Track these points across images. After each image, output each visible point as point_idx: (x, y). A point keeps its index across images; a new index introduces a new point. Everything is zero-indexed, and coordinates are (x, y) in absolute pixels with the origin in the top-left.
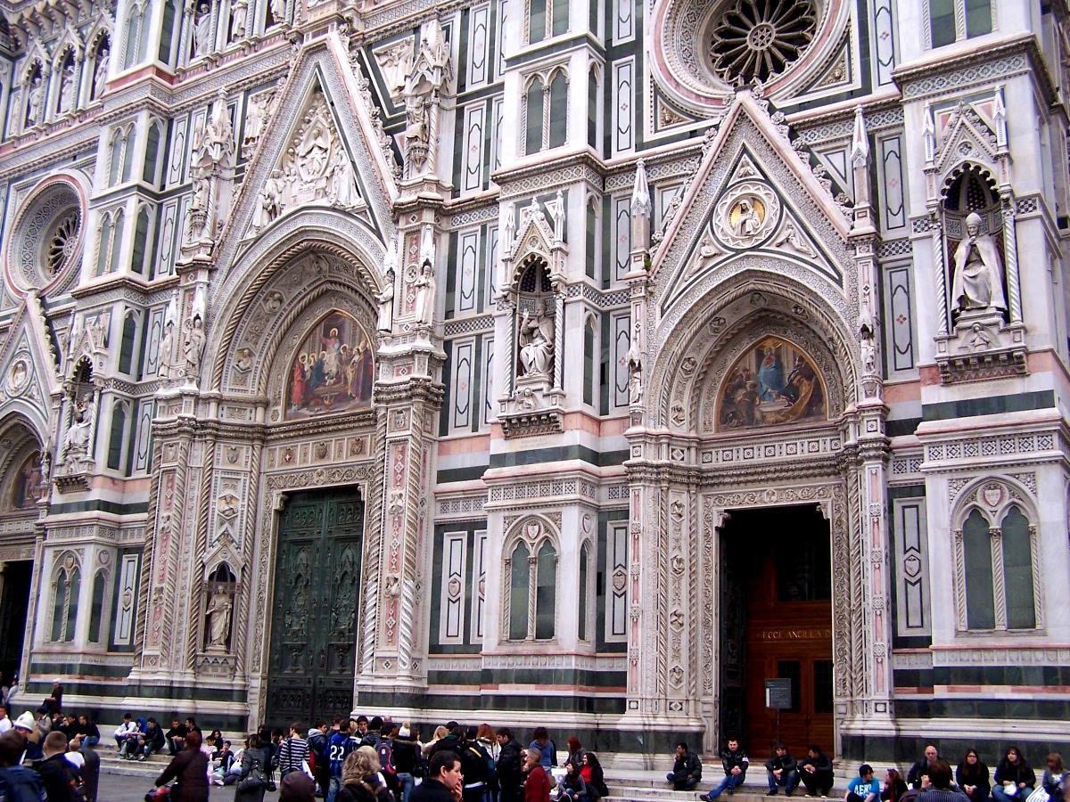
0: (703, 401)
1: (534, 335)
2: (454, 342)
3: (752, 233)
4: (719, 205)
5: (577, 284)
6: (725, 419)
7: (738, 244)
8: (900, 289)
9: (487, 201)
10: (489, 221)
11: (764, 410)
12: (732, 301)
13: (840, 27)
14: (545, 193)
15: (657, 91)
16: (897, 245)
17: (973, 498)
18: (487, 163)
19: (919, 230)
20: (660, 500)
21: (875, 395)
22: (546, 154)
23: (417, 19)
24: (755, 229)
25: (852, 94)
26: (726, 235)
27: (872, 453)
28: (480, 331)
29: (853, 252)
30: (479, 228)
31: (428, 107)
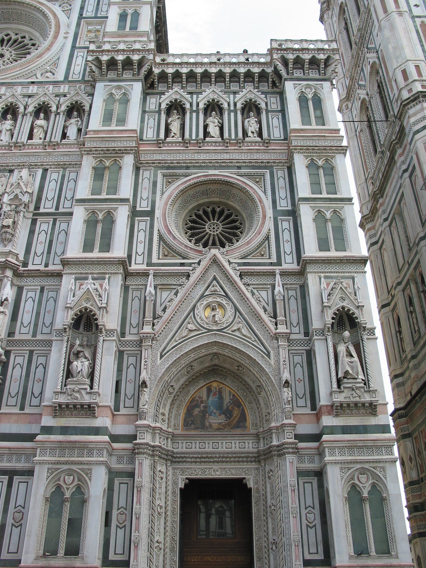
0: (174, 412)
1: (80, 356)
2: (12, 352)
3: (219, 322)
4: (199, 304)
5: (112, 330)
6: (187, 424)
7: (209, 327)
8: (298, 365)
9: (48, 273)
10: (47, 285)
11: (211, 421)
12: (202, 357)
13: (265, 232)
14: (95, 275)
15: (161, 238)
16: (297, 342)
17: (353, 479)
18: (49, 252)
19: (318, 335)
20: (153, 468)
21: (291, 419)
22: (96, 254)
23: (13, 166)
24: (220, 321)
25: (271, 264)
26: (202, 320)
27: (291, 450)
28: (32, 348)
29: (276, 341)
30: (39, 288)
31: (17, 212)
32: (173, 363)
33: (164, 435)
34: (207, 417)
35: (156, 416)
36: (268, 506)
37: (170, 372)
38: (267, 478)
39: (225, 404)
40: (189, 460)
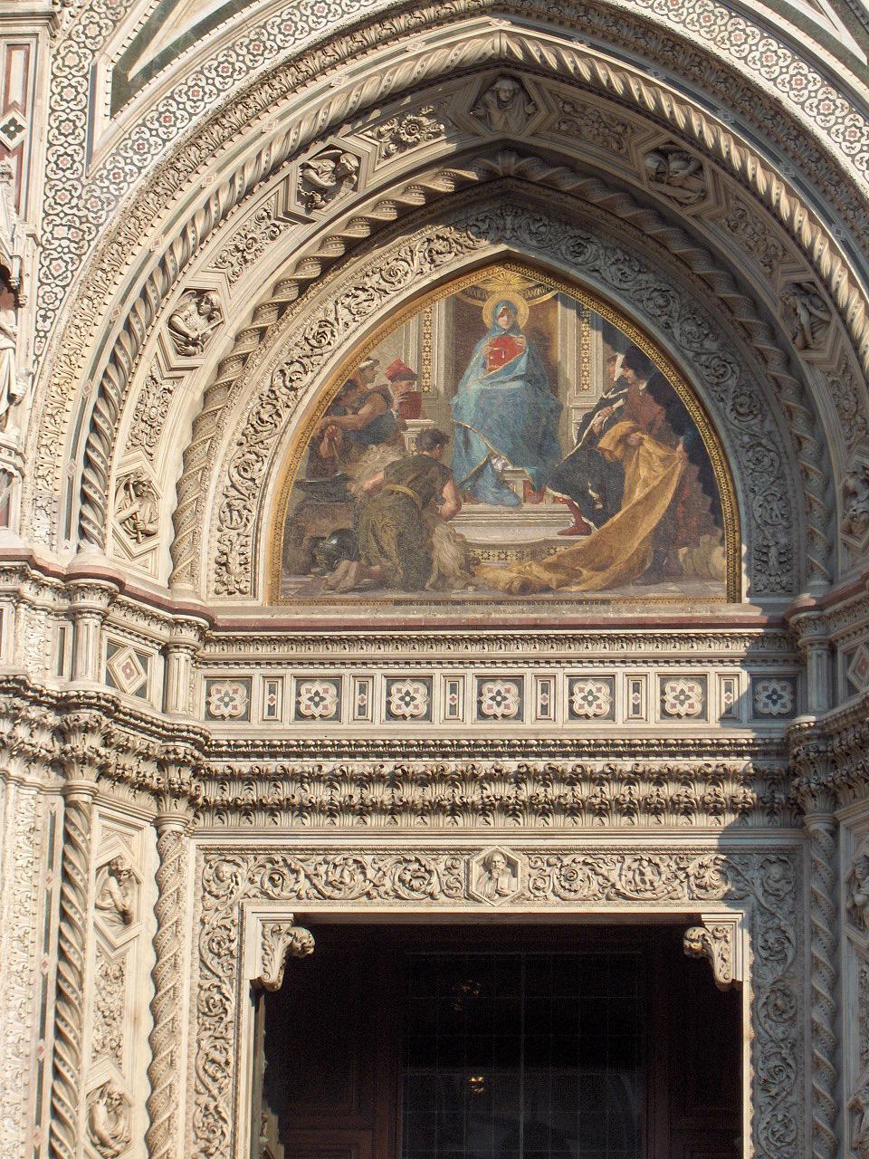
11: (475, 536)
32: (199, 133)
33: (141, 624)
34: (449, 506)
35: (85, 498)
36: (846, 1104)
37: (182, 197)
38: (843, 915)
39: (577, 417)
40: (319, 793)
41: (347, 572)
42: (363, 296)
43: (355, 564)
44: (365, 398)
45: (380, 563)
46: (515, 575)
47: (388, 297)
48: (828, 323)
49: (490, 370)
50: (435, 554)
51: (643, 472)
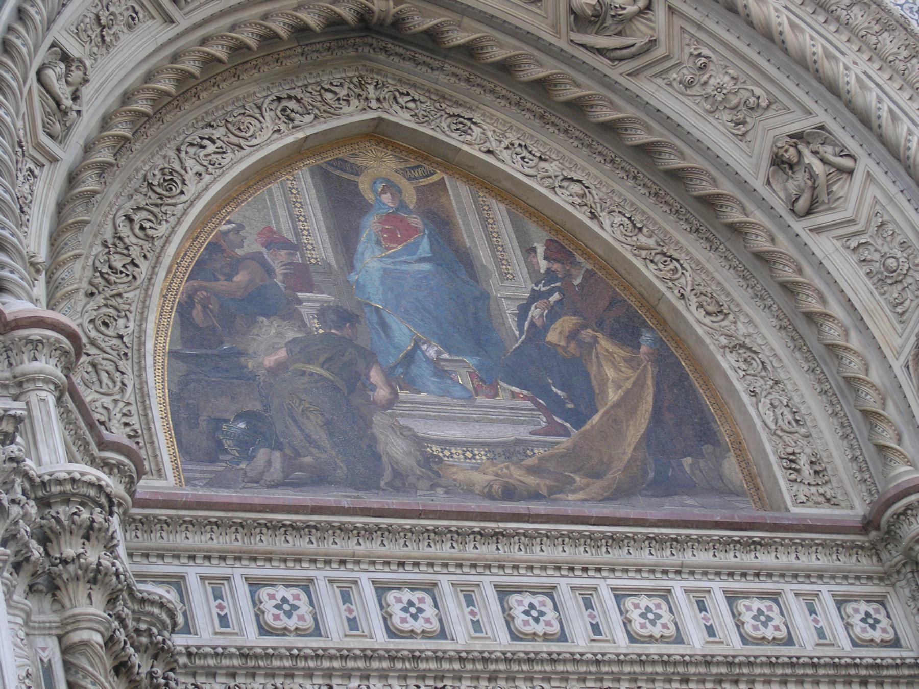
11: (423, 429)
34: (382, 393)
39: (510, 310)
41: (269, 462)
42: (211, 148)
43: (277, 454)
44: (236, 265)
45: (311, 454)
46: (490, 477)
47: (243, 153)
48: (850, 172)
49: (388, 249)
50: (381, 448)
51: (610, 373)
